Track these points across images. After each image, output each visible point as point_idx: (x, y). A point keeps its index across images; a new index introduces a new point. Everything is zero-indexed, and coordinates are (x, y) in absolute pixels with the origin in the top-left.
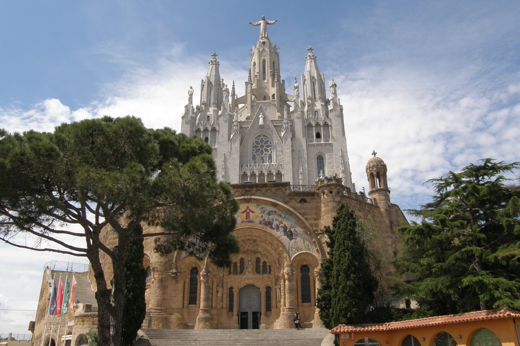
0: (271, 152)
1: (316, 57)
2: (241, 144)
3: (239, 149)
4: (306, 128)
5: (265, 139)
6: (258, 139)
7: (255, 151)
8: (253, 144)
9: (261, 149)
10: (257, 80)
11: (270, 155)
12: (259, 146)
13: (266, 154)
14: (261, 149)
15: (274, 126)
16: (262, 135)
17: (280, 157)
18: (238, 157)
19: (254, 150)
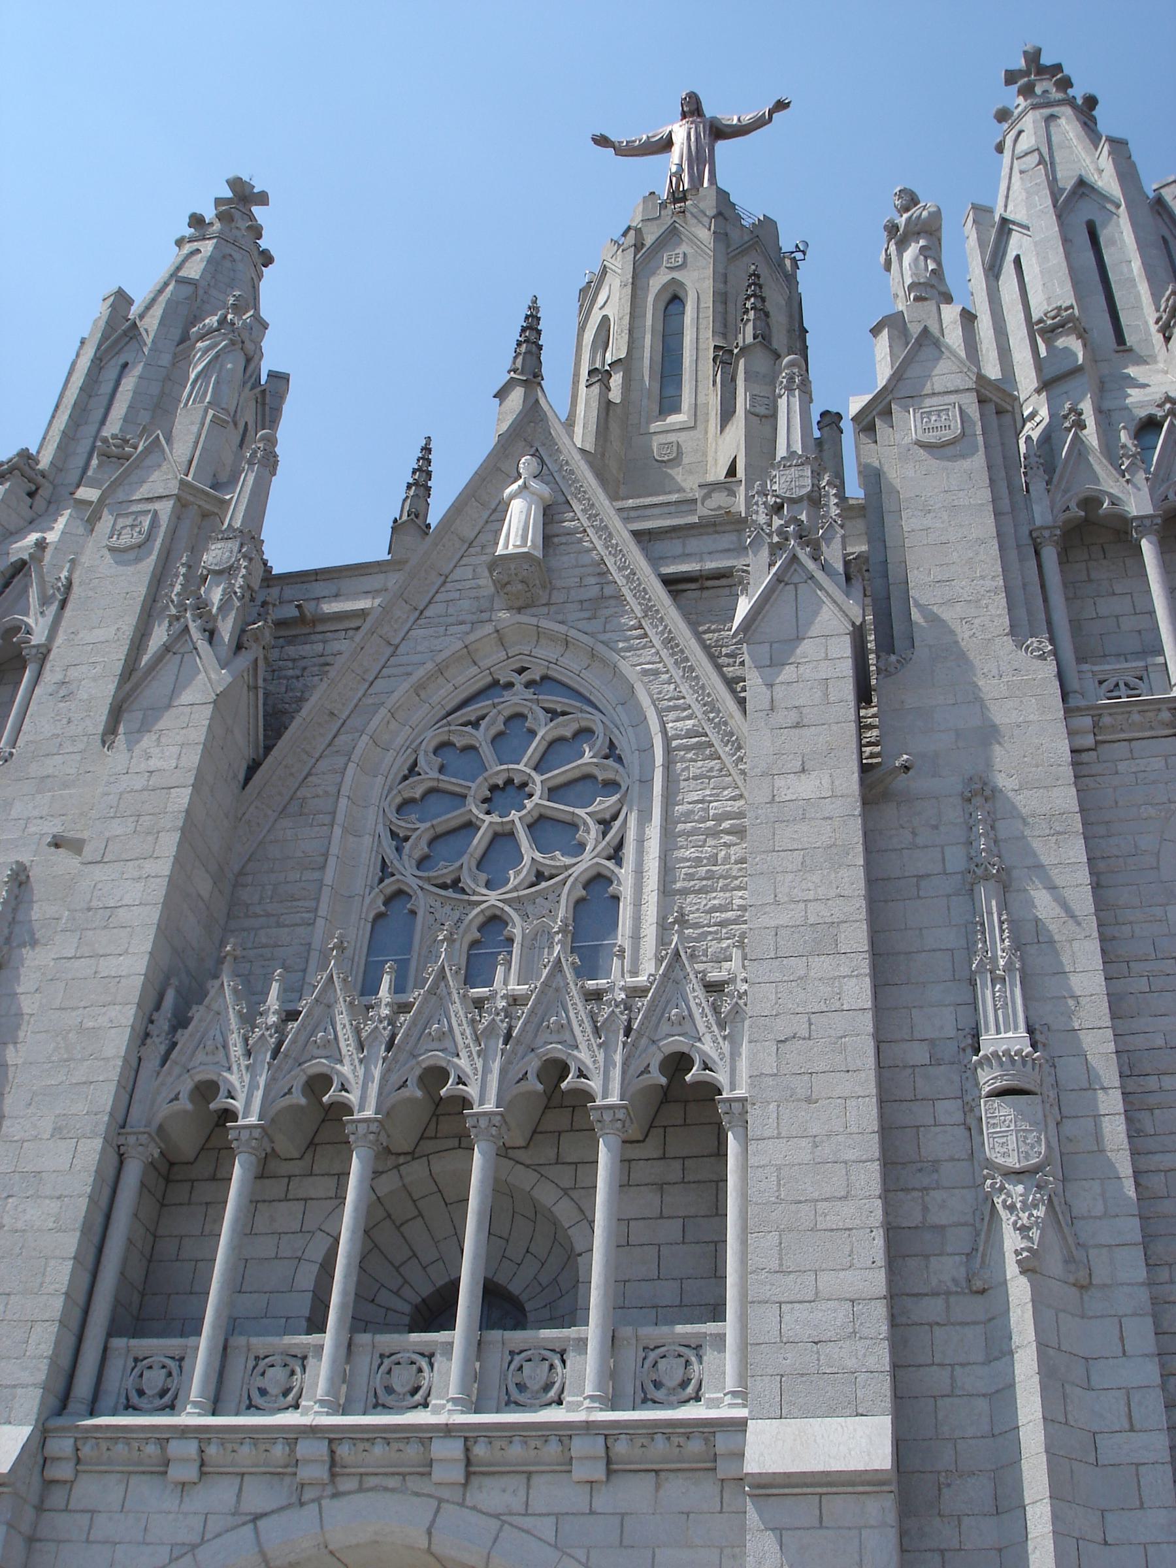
0: (616, 854)
1: (1091, 102)
2: (253, 767)
3: (182, 797)
4: (1050, 555)
5: (553, 714)
6: (475, 724)
7: (417, 847)
8: (413, 770)
9: (488, 821)
10: (607, 406)
11: (599, 881)
12: (478, 788)
13: (540, 876)
14: (488, 821)
15: (672, 583)
16: (519, 680)
17: (718, 898)
18: (158, 890)
19: (399, 839)
